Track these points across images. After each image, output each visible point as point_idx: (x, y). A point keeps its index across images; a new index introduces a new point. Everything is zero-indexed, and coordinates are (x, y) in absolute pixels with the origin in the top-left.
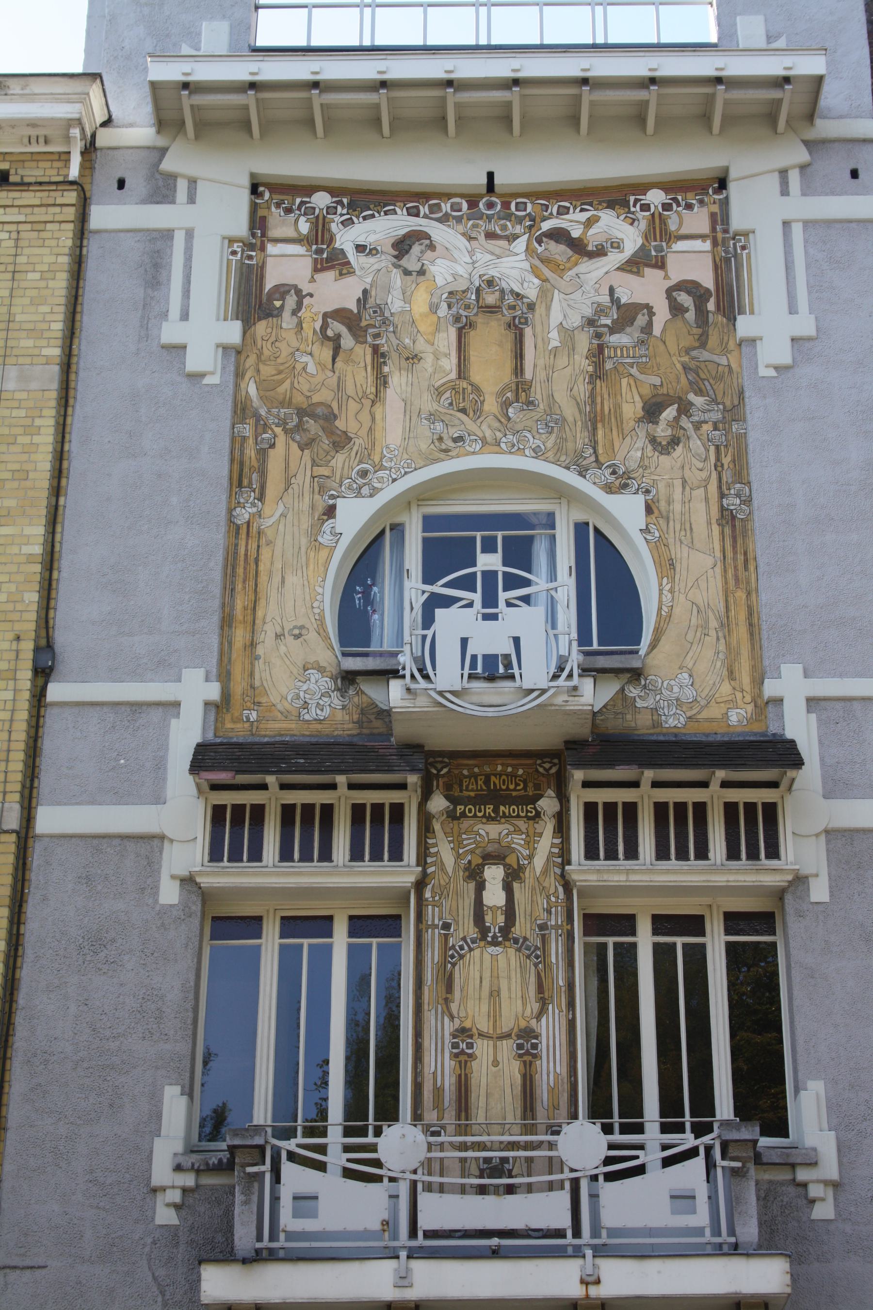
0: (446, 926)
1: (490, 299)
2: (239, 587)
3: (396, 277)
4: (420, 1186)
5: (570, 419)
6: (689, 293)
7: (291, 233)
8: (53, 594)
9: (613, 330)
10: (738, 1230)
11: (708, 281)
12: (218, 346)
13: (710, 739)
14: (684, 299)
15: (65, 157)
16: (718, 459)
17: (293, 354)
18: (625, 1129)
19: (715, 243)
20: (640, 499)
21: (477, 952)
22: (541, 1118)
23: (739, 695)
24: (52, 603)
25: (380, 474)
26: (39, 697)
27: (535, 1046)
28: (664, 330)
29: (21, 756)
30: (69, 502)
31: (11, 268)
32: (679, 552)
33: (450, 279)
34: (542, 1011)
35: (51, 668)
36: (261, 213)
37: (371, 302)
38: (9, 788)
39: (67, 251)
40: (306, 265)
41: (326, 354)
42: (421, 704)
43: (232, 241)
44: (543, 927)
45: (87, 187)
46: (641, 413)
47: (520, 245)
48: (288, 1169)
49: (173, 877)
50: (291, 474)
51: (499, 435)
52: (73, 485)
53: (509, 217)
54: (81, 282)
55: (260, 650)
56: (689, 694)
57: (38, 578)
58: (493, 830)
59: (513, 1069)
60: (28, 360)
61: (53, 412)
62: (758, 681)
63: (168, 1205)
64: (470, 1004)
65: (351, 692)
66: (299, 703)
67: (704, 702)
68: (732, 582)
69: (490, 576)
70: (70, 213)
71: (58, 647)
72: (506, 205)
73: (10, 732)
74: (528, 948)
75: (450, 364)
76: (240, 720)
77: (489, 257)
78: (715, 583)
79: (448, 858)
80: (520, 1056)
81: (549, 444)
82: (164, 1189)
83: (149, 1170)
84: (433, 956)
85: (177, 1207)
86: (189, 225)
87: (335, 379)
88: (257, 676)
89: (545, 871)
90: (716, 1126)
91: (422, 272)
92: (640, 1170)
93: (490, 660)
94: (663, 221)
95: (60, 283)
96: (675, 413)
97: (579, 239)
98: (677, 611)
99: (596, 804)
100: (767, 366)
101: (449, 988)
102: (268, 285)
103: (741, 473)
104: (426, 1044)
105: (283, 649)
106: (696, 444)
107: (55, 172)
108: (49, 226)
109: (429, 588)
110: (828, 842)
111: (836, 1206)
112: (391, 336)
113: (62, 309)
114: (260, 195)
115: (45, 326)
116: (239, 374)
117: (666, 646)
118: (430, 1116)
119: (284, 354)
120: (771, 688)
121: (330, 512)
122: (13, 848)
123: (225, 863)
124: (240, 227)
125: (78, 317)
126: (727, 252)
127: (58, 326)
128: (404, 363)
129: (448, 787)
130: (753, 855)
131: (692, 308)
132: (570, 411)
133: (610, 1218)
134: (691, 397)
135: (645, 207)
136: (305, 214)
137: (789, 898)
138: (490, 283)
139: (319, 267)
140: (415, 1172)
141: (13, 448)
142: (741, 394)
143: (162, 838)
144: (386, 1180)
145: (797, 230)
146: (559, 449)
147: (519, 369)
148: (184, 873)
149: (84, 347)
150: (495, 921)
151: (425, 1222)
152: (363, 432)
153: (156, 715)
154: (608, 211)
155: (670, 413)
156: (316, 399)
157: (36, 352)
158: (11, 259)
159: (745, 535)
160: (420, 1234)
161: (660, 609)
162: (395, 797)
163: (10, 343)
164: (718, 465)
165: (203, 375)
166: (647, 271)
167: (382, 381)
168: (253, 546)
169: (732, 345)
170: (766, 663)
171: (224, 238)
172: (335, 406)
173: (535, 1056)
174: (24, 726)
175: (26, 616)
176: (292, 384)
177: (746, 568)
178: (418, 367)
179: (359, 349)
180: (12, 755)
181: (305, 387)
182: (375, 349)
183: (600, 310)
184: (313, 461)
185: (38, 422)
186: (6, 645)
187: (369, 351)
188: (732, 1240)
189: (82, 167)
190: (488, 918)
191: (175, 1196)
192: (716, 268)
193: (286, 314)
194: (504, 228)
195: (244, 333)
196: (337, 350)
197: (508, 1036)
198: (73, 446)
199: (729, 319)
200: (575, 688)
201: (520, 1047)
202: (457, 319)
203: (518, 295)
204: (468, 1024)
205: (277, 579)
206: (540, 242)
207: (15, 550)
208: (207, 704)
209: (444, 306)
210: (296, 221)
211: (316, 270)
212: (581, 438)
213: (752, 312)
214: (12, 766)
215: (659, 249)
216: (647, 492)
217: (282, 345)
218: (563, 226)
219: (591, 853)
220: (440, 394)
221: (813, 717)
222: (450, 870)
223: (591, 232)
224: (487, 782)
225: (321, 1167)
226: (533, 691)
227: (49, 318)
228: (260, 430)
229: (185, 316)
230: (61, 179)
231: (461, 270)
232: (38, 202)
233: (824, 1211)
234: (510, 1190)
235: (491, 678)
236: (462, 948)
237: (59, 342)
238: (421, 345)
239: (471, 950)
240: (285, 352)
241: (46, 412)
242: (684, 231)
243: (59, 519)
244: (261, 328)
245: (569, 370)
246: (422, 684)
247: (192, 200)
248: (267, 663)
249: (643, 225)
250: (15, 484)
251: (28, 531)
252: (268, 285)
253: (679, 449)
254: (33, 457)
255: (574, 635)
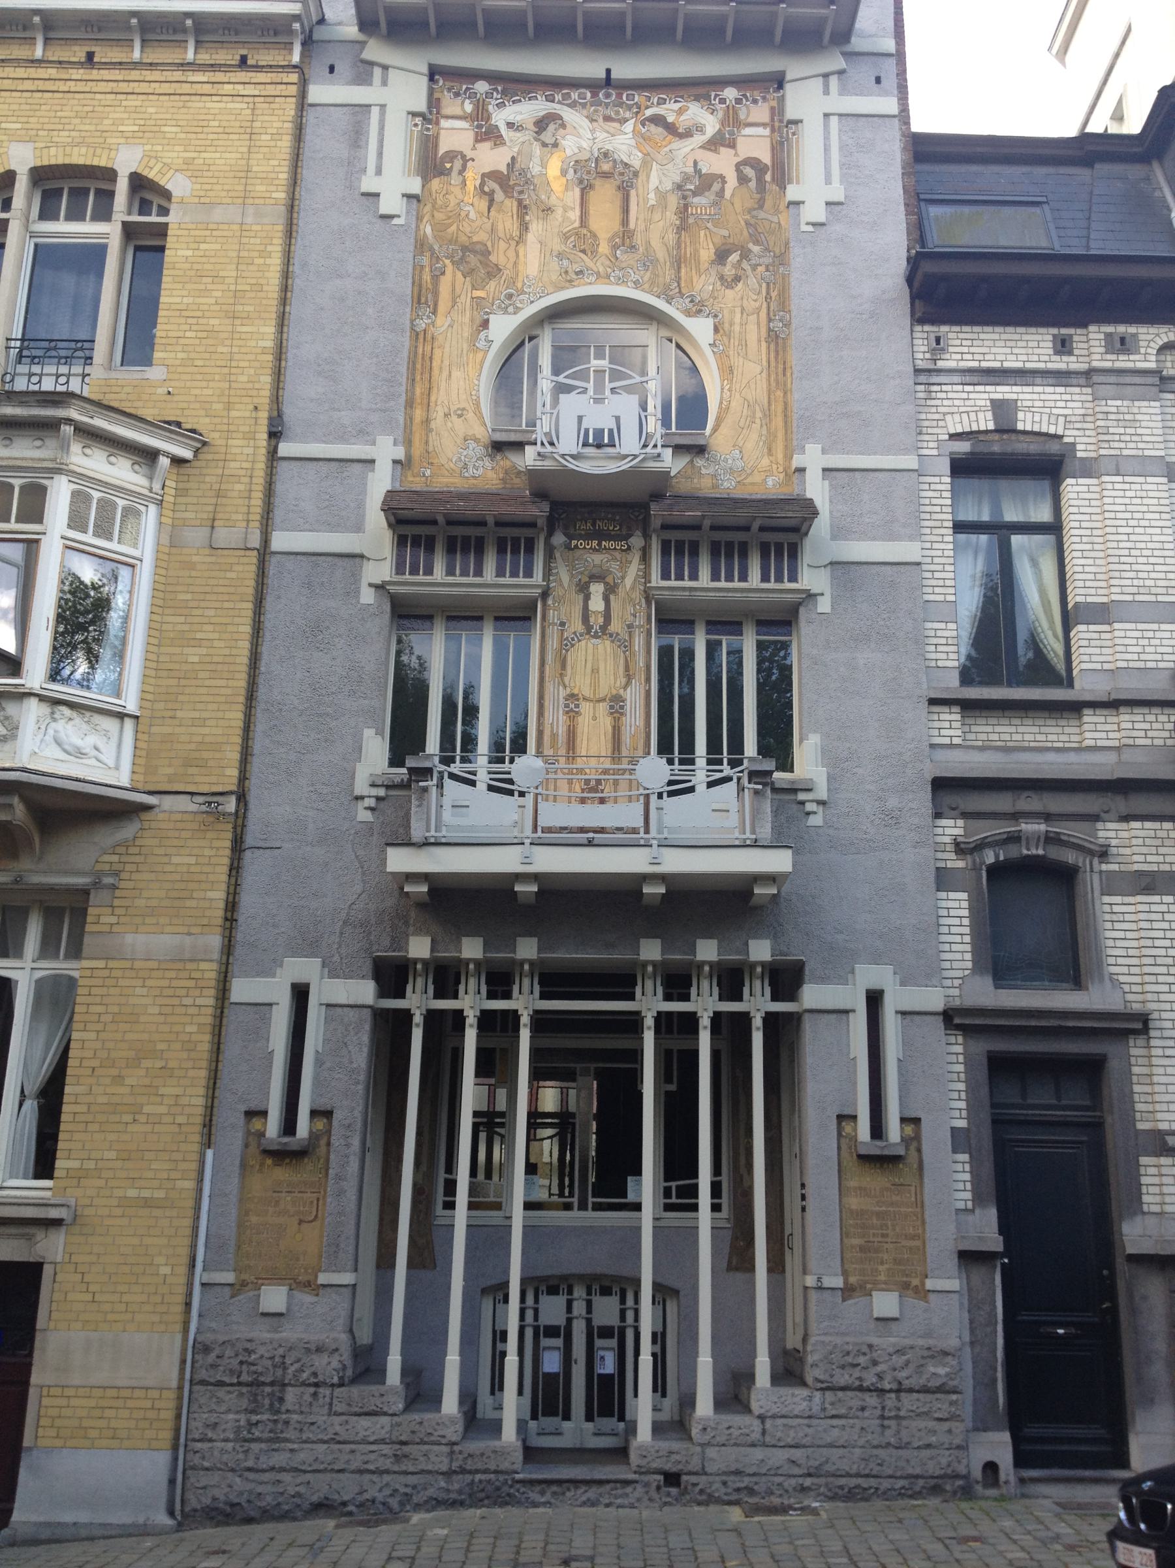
0: (563, 624)
1: (606, 167)
2: (418, 378)
3: (537, 149)
4: (540, 797)
5: (662, 260)
6: (752, 167)
7: (458, 112)
8: (282, 378)
9: (695, 193)
10: (758, 830)
11: (766, 158)
12: (403, 195)
13: (754, 497)
14: (749, 172)
15: (289, 46)
16: (768, 293)
17: (459, 204)
18: (682, 762)
19: (773, 130)
20: (709, 323)
21: (583, 643)
22: (624, 752)
23: (775, 466)
24: (281, 385)
25: (521, 297)
26: (273, 454)
27: (622, 707)
28: (733, 195)
29: (260, 495)
30: (293, 310)
31: (249, 130)
32: (737, 362)
33: (576, 151)
34: (628, 683)
35: (281, 432)
36: (436, 95)
37: (517, 166)
38: (251, 517)
39: (290, 119)
40: (470, 136)
41: (483, 204)
42: (548, 464)
43: (414, 114)
44: (630, 626)
45: (306, 71)
46: (713, 257)
47: (629, 127)
48: (447, 782)
49: (370, 585)
50: (458, 291)
51: (609, 270)
52: (295, 298)
53: (621, 105)
54: (302, 145)
55: (433, 425)
56: (740, 464)
57: (270, 365)
58: (597, 558)
59: (606, 722)
60: (262, 201)
61: (280, 241)
62: (789, 457)
63: (366, 808)
64: (577, 677)
65: (498, 458)
66: (461, 465)
67: (749, 471)
68: (773, 384)
69: (599, 372)
70: (293, 90)
71: (285, 419)
72: (619, 96)
73: (251, 477)
74: (619, 640)
75: (575, 215)
76: (418, 475)
77: (606, 135)
78: (762, 385)
79: (565, 578)
80: (612, 713)
81: (646, 278)
82: (362, 798)
83: (352, 785)
84: (553, 643)
85: (372, 809)
86: (382, 102)
87: (489, 225)
88: (431, 443)
89: (633, 588)
90: (745, 761)
91: (555, 145)
92: (691, 790)
93: (599, 433)
94: (735, 113)
95: (286, 143)
96: (738, 258)
97: (673, 124)
98: (733, 404)
99: (670, 541)
100: (807, 224)
101: (563, 666)
102: (441, 152)
103: (784, 305)
104: (546, 704)
105: (449, 424)
106: (752, 281)
107: (281, 58)
108: (277, 99)
109: (555, 378)
110: (832, 571)
111: (824, 817)
112: (532, 193)
113: (287, 163)
114: (437, 82)
115: (273, 175)
116: (419, 219)
117: (724, 430)
118: (548, 751)
119: (452, 204)
120: (797, 461)
121: (485, 324)
122: (255, 561)
123: (407, 576)
124: (422, 106)
125: (299, 170)
126: (781, 137)
127: (284, 176)
128: (540, 213)
129: (566, 527)
130: (779, 579)
131: (754, 179)
132: (661, 254)
133: (668, 820)
134: (751, 246)
135: (722, 101)
136: (469, 98)
137: (802, 610)
138: (606, 155)
139: (479, 138)
140: (537, 788)
141: (251, 268)
142: (787, 243)
143: (362, 556)
144: (516, 794)
145: (834, 120)
146: (652, 283)
147: (625, 222)
148: (377, 581)
149: (302, 193)
150: (597, 621)
151: (541, 823)
152: (510, 266)
153: (357, 467)
154: (696, 103)
155: (734, 257)
156: (475, 239)
157: (268, 195)
158: (249, 124)
159: (784, 351)
160: (539, 829)
161: (721, 403)
162: (528, 532)
163: (249, 188)
164: (768, 298)
165: (392, 217)
166: (723, 150)
167: (524, 227)
168: (428, 348)
169: (782, 207)
170: (795, 443)
171: (409, 113)
172: (489, 244)
173: (622, 714)
174: (262, 473)
175: (263, 393)
176: (458, 229)
177: (784, 375)
178: (551, 217)
179: (508, 202)
180: (254, 494)
181: (467, 229)
182: (520, 202)
183: (686, 178)
184: (473, 286)
185: (269, 248)
186: (248, 414)
187: (515, 204)
188: (754, 837)
189: (302, 55)
190: (592, 620)
191: (371, 802)
192: (773, 148)
193: (454, 173)
194: (617, 113)
195: (423, 186)
196: (491, 202)
197: (603, 700)
198: (296, 268)
199: (780, 188)
200: (659, 455)
201: (611, 707)
202: (581, 181)
203: (626, 164)
204: (576, 691)
205: (445, 374)
206: (643, 125)
207: (253, 343)
208: (395, 462)
209: (571, 171)
210: (463, 103)
211: (477, 141)
212: (668, 274)
213: (798, 182)
214: (253, 502)
215: (732, 133)
216: (716, 316)
217: (451, 197)
218: (662, 113)
219: (665, 576)
220: (567, 238)
221: (827, 482)
222: (566, 585)
223: (682, 118)
224: (594, 525)
225: (473, 783)
226: (628, 456)
227: (277, 169)
228: (434, 260)
229: (379, 172)
230: (286, 63)
231: (585, 145)
232: (269, 81)
233: (816, 820)
234: (602, 801)
235: (599, 446)
236: (573, 639)
237: (284, 188)
238: (553, 200)
239: (579, 641)
240: (453, 202)
241: (275, 241)
242: (750, 120)
243: (286, 322)
244: (435, 184)
245: (661, 223)
246: (549, 448)
247: (384, 83)
248: (438, 434)
249: (720, 114)
250: (253, 295)
251: (263, 329)
252: (441, 152)
253: (740, 285)
254: (267, 274)
255: (659, 416)
